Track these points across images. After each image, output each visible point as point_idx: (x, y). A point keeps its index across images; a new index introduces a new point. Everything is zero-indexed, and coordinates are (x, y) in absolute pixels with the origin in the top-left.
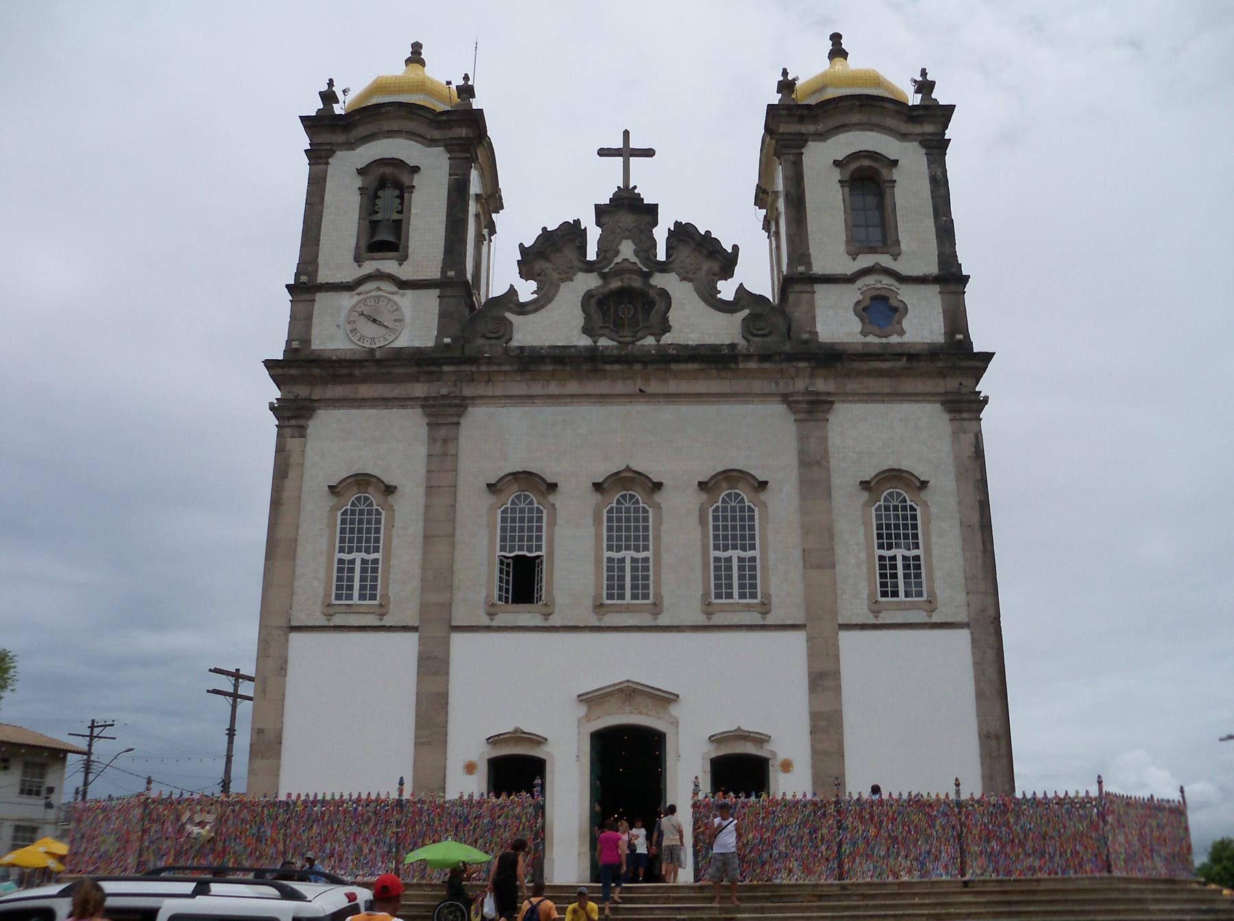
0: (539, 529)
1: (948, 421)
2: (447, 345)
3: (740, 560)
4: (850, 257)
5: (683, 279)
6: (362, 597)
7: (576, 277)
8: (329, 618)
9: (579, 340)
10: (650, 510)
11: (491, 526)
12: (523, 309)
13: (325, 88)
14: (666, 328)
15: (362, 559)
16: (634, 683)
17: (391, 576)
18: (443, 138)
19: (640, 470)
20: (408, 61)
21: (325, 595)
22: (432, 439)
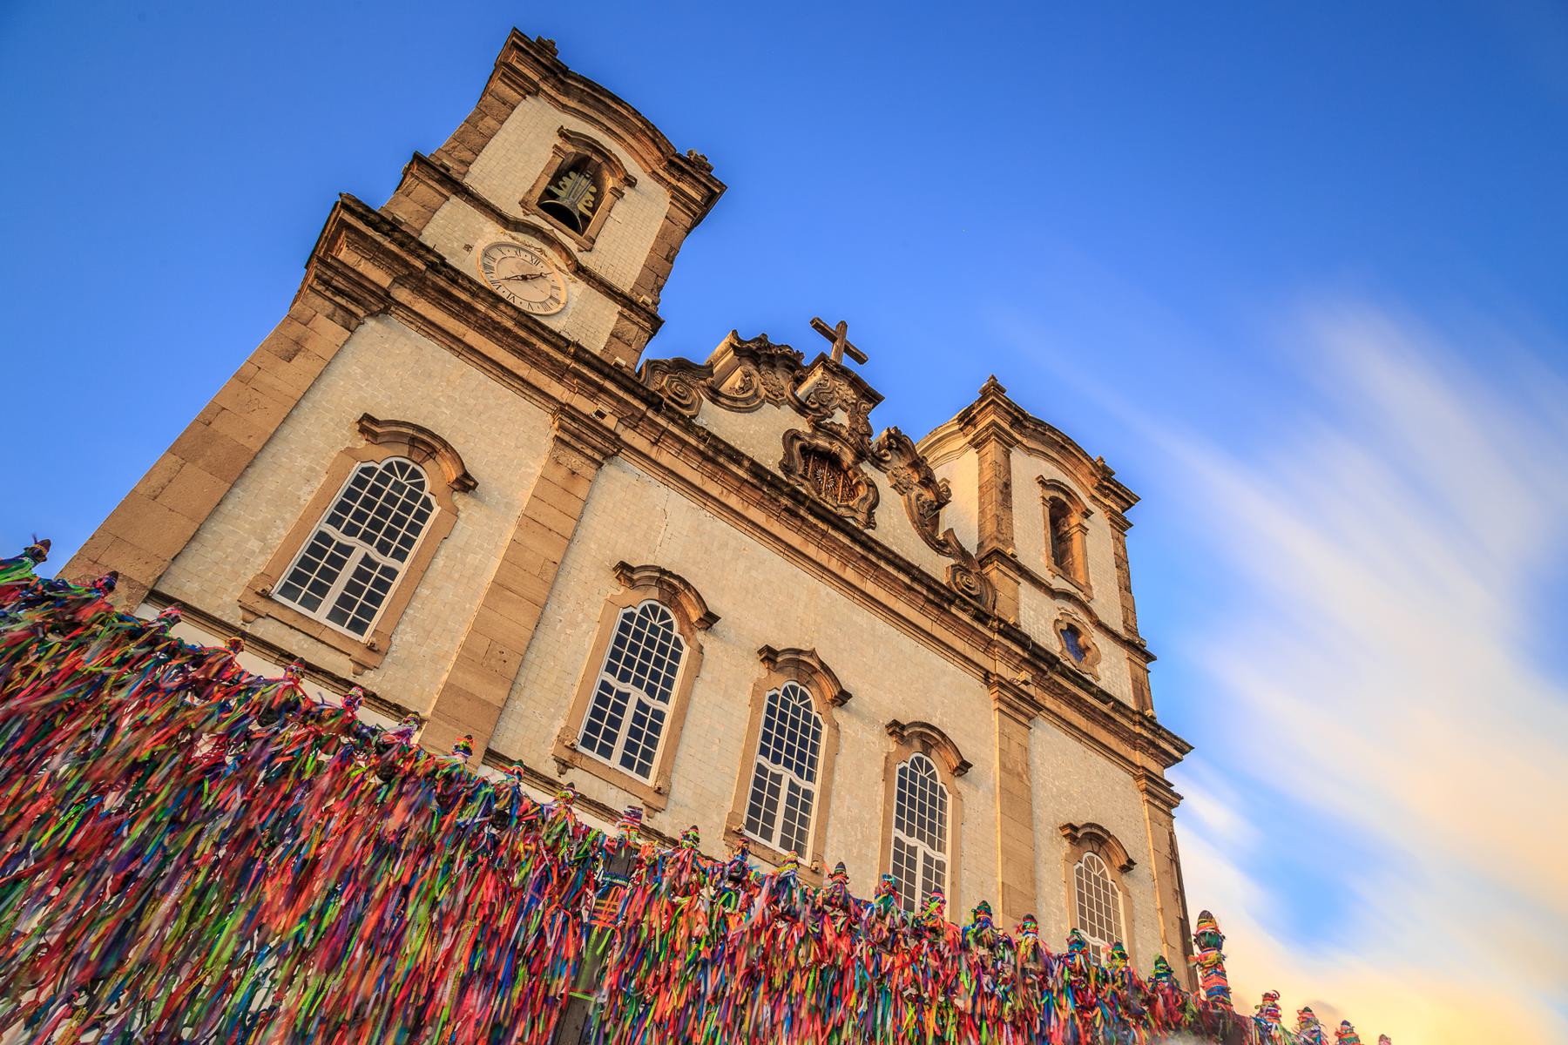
0: (672, 670)
5: (894, 487)
6: (336, 615)
8: (251, 618)
12: (715, 395)
15: (366, 555)
17: (410, 611)
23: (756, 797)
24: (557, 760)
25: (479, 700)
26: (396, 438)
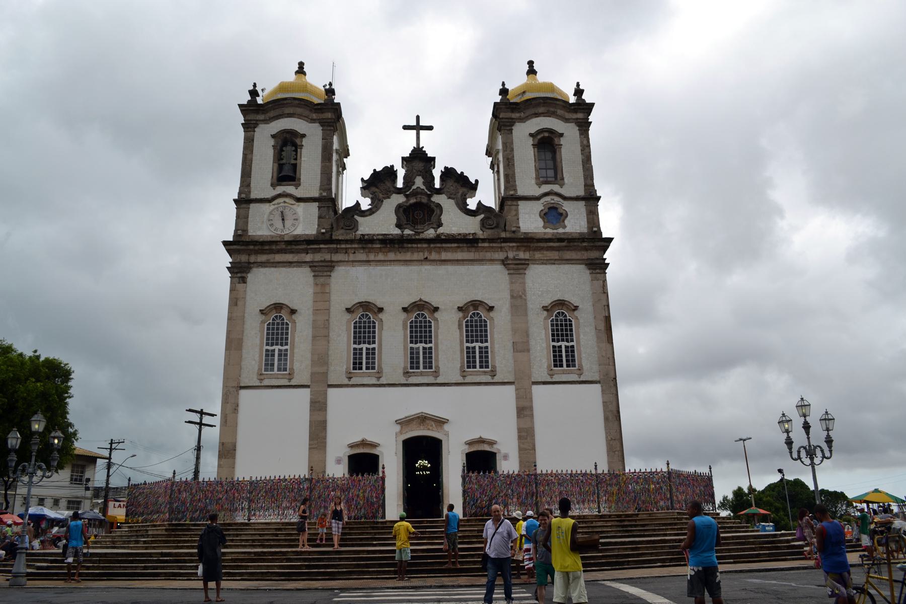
0: (374, 332)
1: (589, 274)
2: (323, 233)
3: (480, 348)
4: (537, 186)
5: (449, 198)
7: (392, 197)
8: (261, 381)
9: (394, 231)
10: (433, 322)
11: (348, 330)
12: (364, 214)
13: (252, 88)
14: (440, 225)
16: (425, 413)
18: (318, 118)
19: (427, 301)
20: (297, 72)
21: (259, 369)
22: (316, 284)
23: (412, 358)
24: (347, 378)
25: (321, 373)
26: (271, 310)
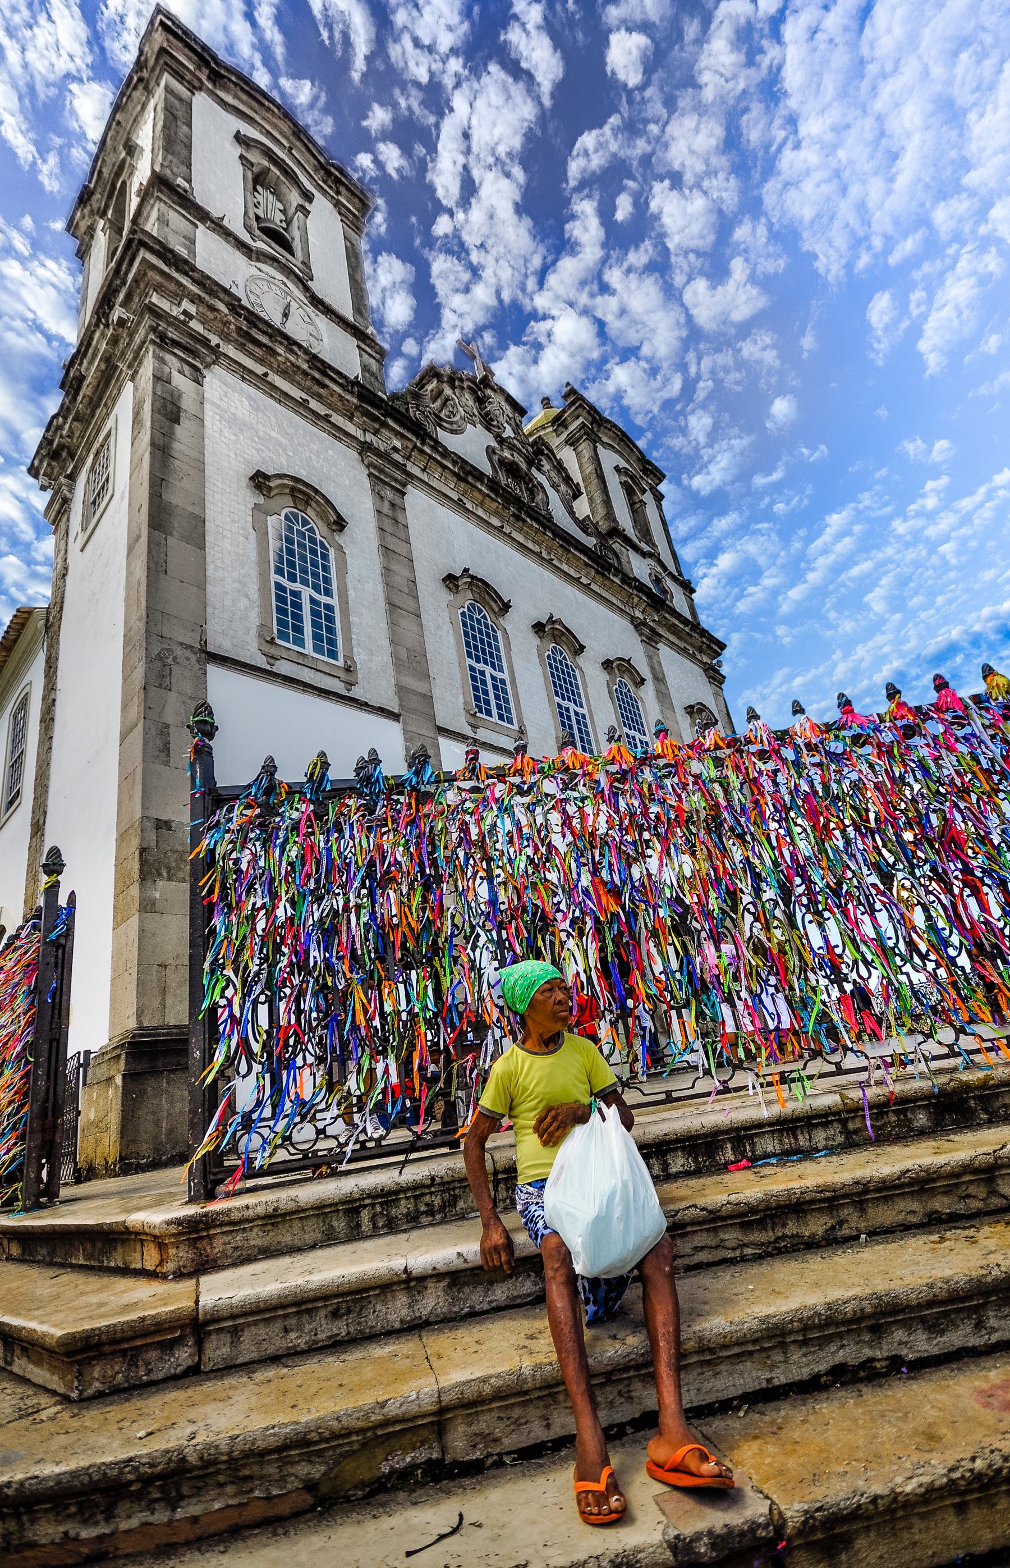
8: (272, 661)
